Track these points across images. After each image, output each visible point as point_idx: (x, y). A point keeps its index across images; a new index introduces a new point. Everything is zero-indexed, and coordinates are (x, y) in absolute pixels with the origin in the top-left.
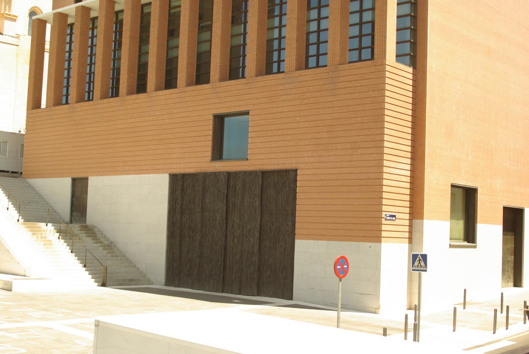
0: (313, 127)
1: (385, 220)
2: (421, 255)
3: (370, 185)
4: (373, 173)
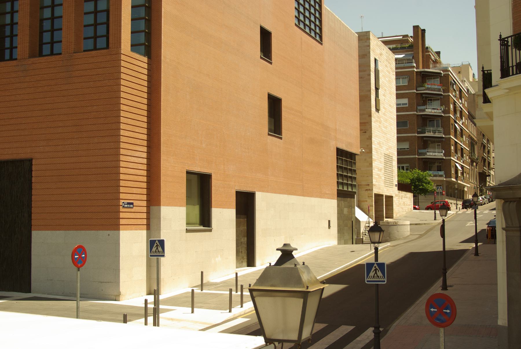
0: (48, 116)
1: (123, 208)
2: (158, 240)
3: (107, 174)
4: (110, 161)
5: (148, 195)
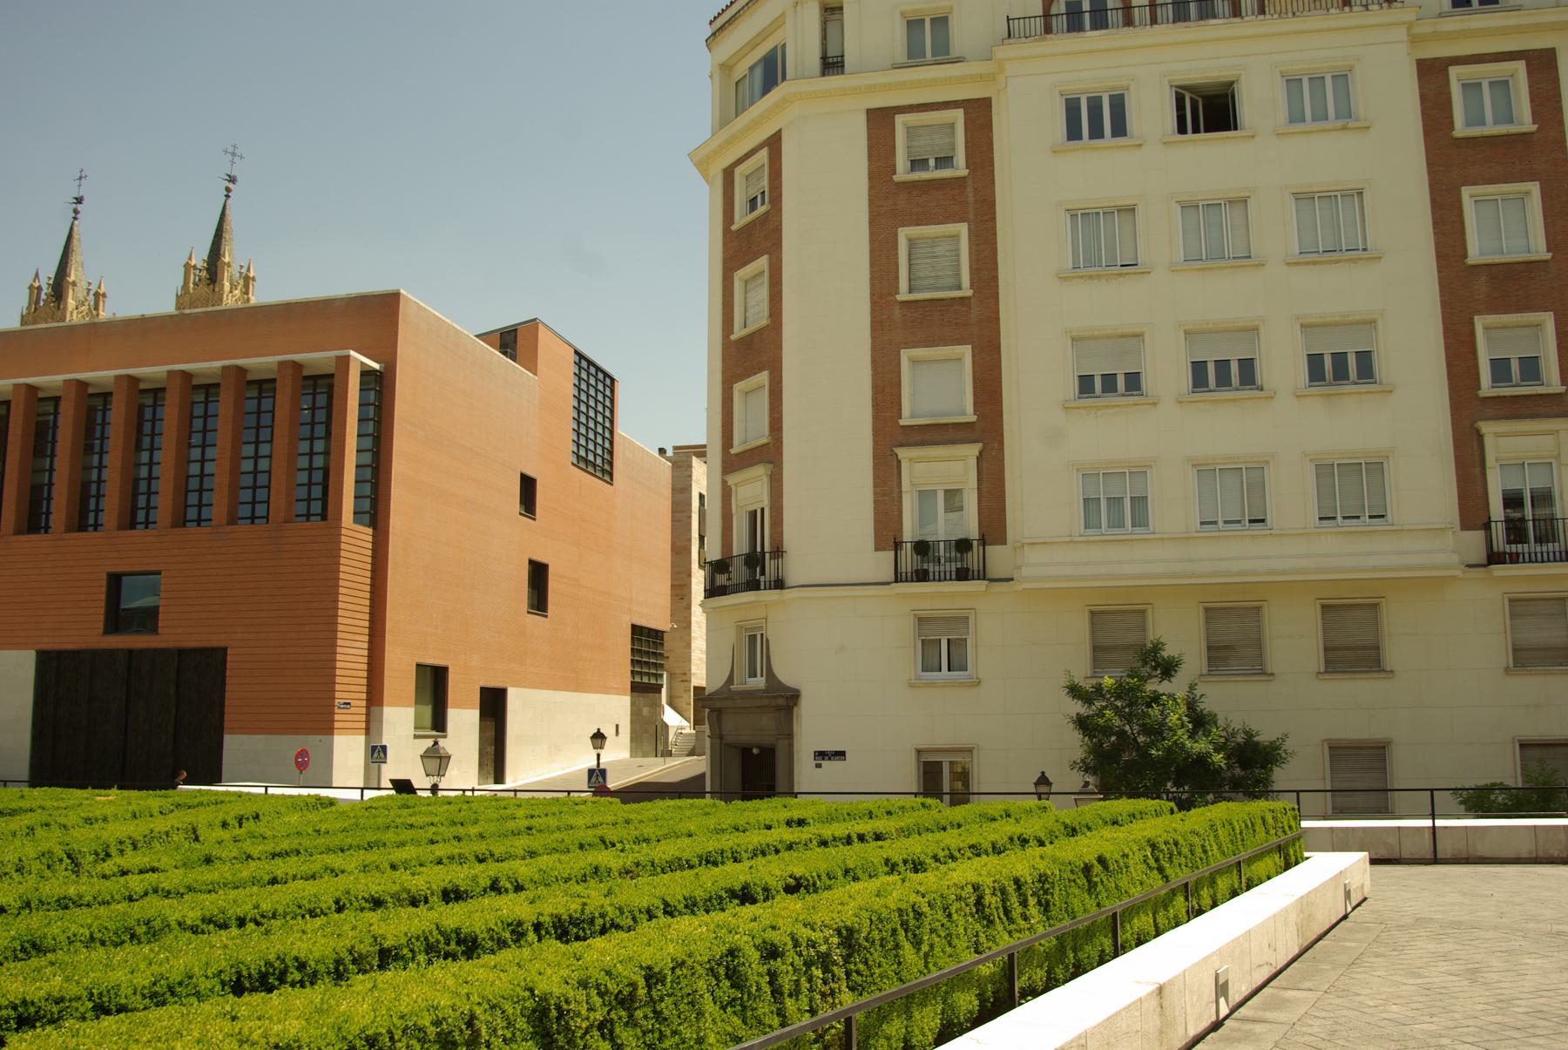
5: (368, 693)
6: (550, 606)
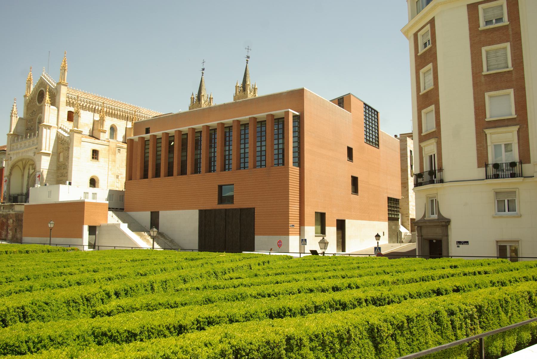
5: (300, 222)
6: (359, 192)
